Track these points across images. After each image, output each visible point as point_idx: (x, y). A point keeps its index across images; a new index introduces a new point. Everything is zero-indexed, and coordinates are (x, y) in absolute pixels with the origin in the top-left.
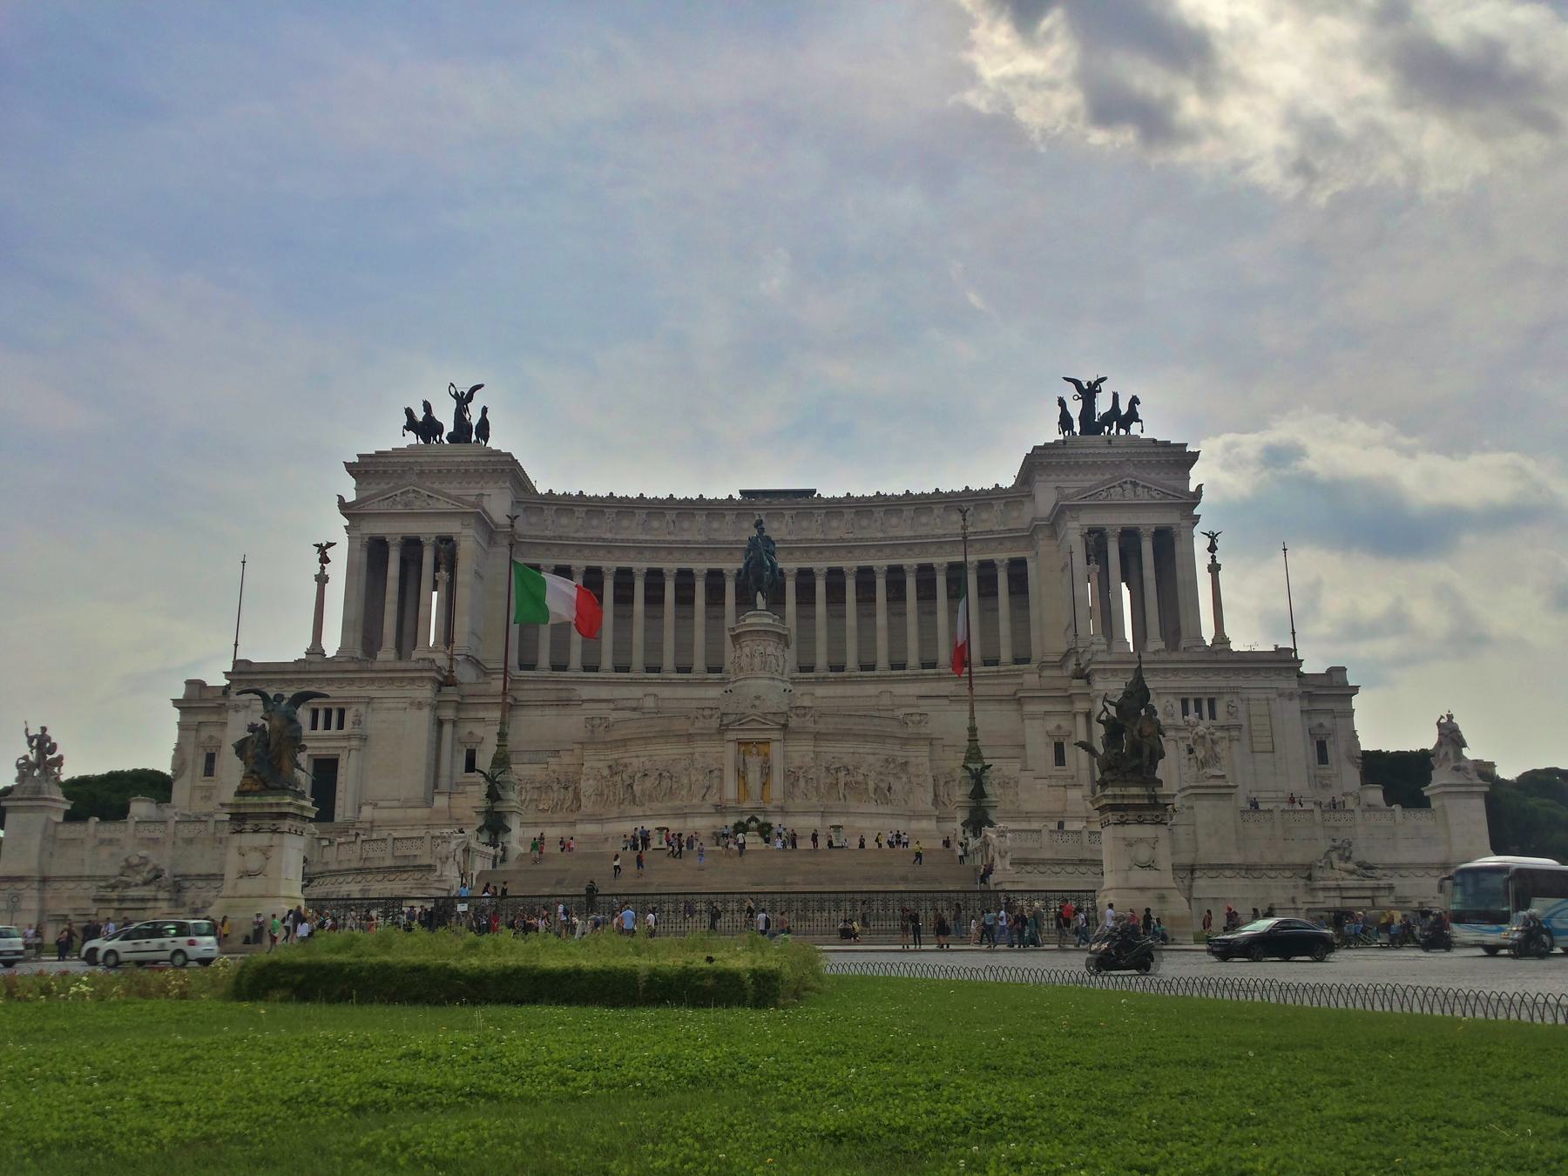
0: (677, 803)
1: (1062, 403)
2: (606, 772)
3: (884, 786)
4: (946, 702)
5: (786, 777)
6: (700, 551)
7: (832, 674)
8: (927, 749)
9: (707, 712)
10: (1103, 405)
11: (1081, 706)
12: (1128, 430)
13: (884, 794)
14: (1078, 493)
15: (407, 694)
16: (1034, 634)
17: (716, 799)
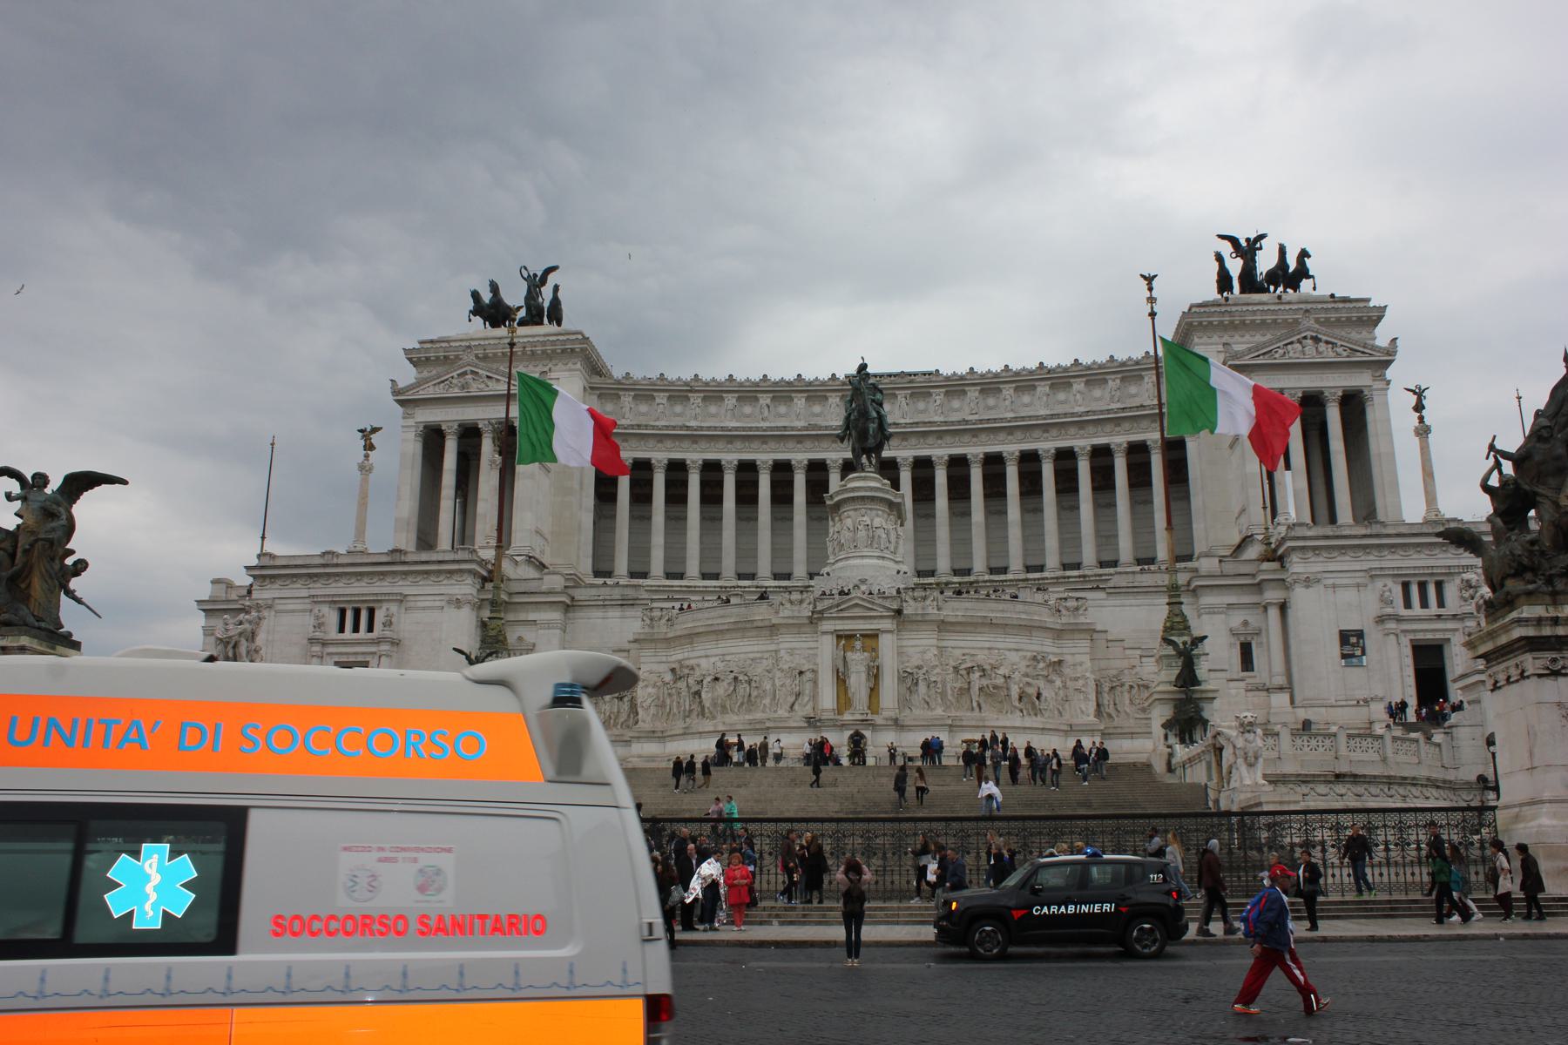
0: (759, 715)
1: (1219, 258)
2: (668, 677)
3: (1032, 691)
4: (1102, 595)
5: (901, 679)
6: (800, 439)
7: (956, 579)
8: (1087, 643)
9: (796, 596)
10: (1266, 262)
11: (1273, 595)
12: (1296, 288)
13: (1031, 701)
14: (1250, 350)
15: (443, 590)
16: (1198, 527)
17: (808, 711)
